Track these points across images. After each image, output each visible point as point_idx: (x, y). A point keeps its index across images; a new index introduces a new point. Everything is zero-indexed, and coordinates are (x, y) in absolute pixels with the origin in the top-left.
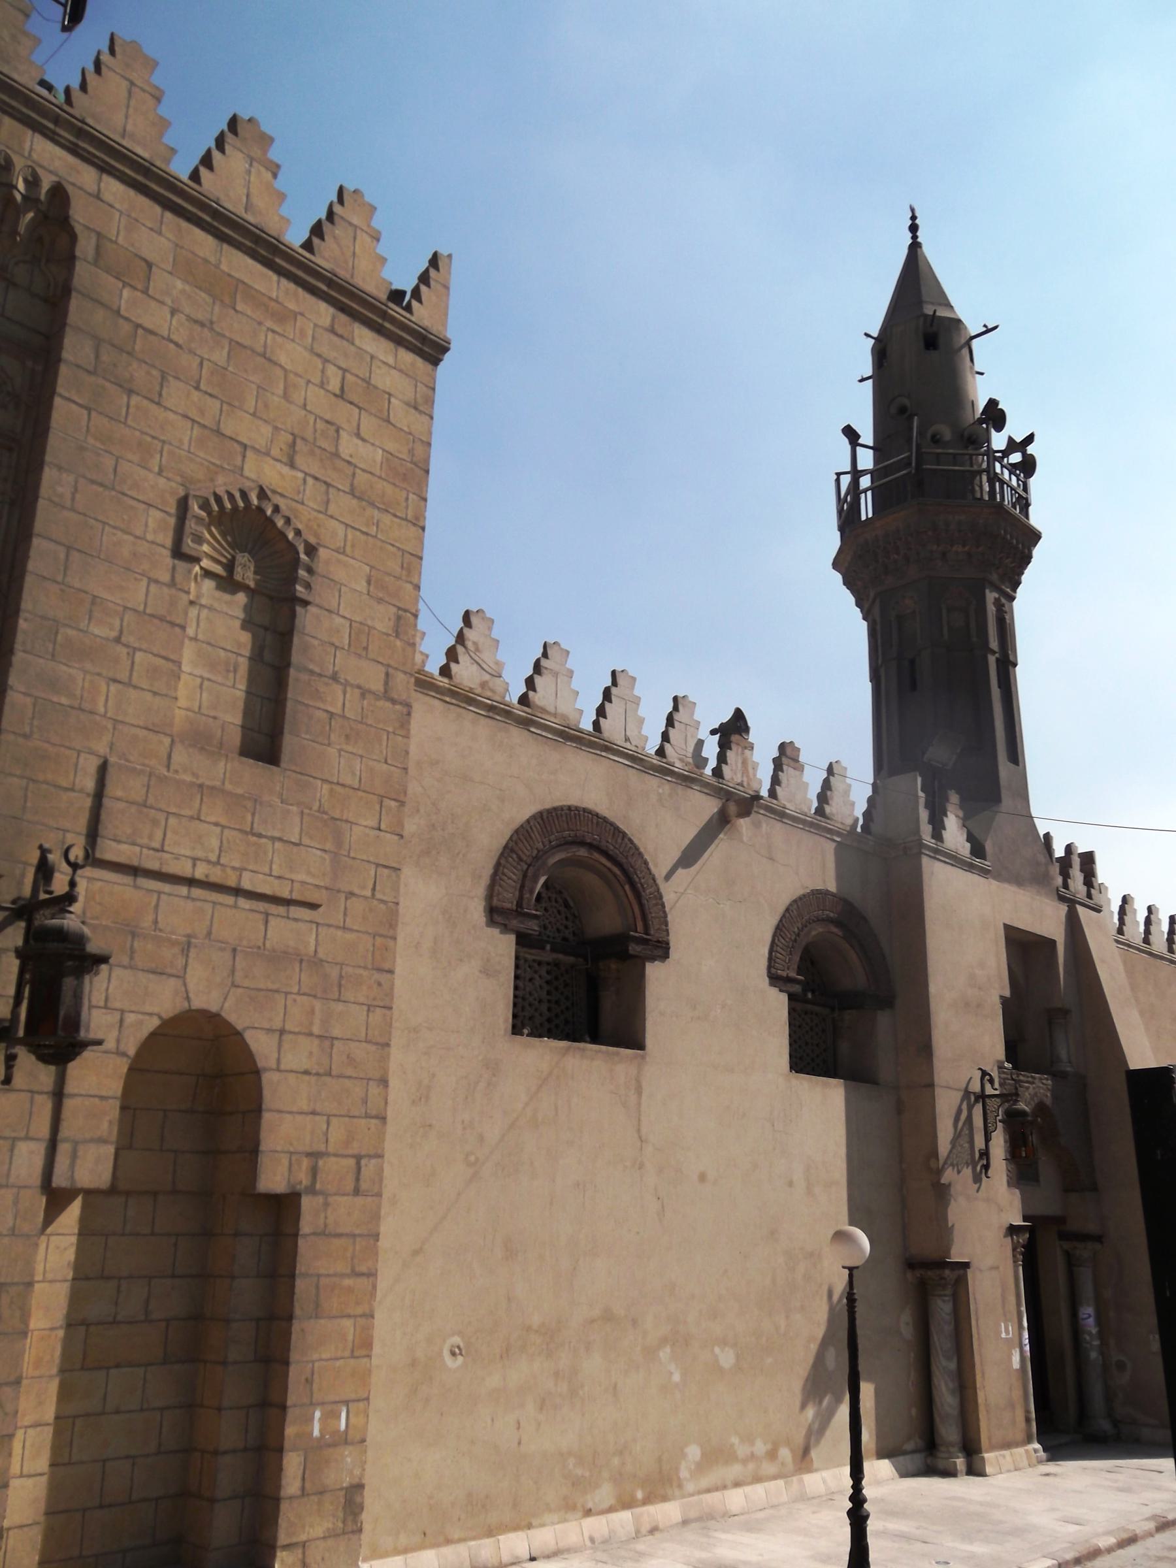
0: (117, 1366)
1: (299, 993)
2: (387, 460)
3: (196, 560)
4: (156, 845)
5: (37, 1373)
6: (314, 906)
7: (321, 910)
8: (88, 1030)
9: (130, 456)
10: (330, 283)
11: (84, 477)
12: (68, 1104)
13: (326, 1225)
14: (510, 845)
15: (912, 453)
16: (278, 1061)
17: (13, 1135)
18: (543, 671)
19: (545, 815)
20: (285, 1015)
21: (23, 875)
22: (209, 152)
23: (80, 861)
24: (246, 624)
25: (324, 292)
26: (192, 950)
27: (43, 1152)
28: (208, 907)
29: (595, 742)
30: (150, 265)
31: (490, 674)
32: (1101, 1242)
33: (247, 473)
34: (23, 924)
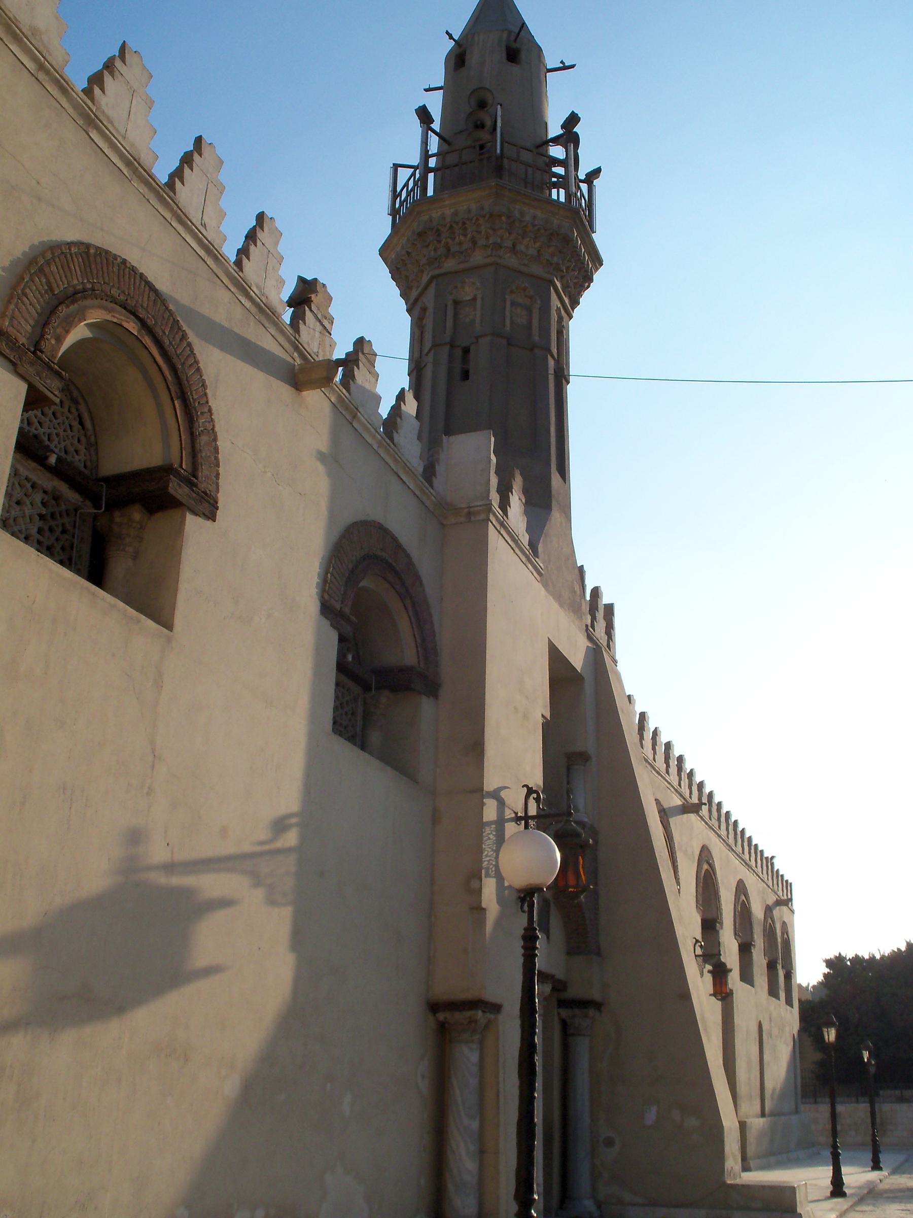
19: (92, 251)
32: (600, 1011)
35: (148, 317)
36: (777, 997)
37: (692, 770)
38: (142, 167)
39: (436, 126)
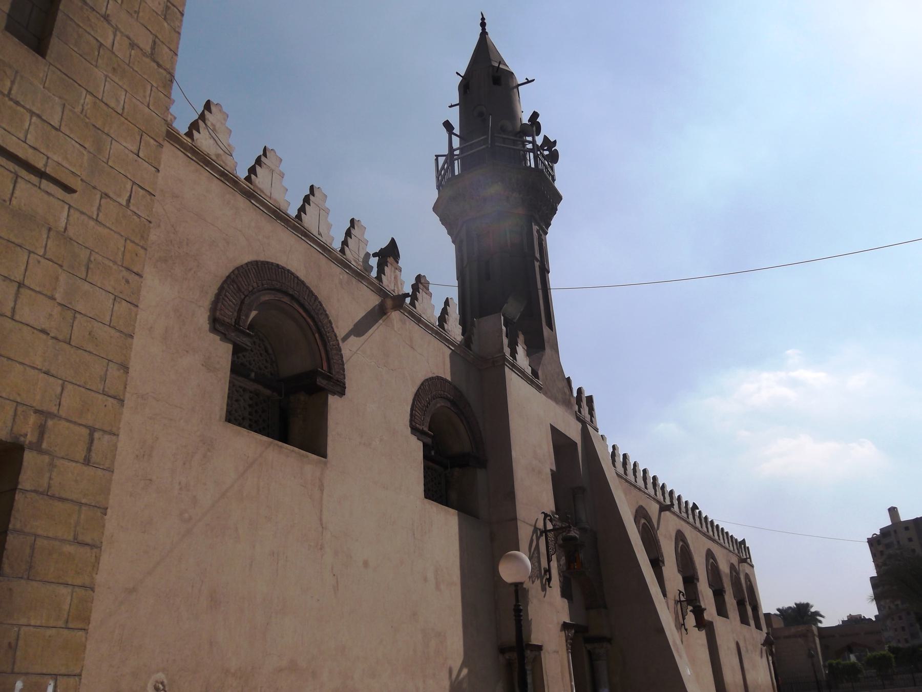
1: (43, 256)
6: (69, 190)
7: (75, 195)
13: (49, 486)
14: (232, 277)
15: (488, 136)
16: (14, 309)
18: (263, 164)
19: (259, 263)
20: (26, 270)
29: (298, 226)
31: (224, 151)
35: (295, 293)
36: (748, 624)
37: (663, 484)
38: (282, 212)
39: (457, 130)
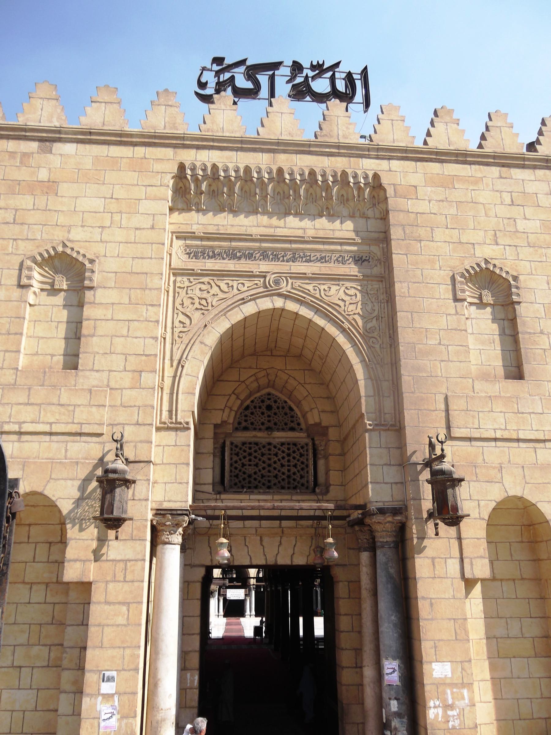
0: (514, 657)
2: (543, 224)
3: (465, 300)
4: (477, 427)
5: (478, 658)
8: (462, 511)
9: (426, 267)
10: (494, 157)
11: (411, 282)
12: (464, 542)
17: (445, 557)
21: (425, 449)
22: (428, 130)
23: (443, 440)
24: (494, 320)
25: (492, 162)
26: (503, 470)
27: (458, 563)
28: (506, 449)
30: (415, 187)
33: (477, 256)
34: (429, 469)
